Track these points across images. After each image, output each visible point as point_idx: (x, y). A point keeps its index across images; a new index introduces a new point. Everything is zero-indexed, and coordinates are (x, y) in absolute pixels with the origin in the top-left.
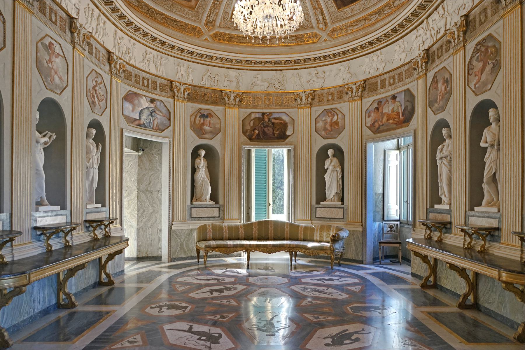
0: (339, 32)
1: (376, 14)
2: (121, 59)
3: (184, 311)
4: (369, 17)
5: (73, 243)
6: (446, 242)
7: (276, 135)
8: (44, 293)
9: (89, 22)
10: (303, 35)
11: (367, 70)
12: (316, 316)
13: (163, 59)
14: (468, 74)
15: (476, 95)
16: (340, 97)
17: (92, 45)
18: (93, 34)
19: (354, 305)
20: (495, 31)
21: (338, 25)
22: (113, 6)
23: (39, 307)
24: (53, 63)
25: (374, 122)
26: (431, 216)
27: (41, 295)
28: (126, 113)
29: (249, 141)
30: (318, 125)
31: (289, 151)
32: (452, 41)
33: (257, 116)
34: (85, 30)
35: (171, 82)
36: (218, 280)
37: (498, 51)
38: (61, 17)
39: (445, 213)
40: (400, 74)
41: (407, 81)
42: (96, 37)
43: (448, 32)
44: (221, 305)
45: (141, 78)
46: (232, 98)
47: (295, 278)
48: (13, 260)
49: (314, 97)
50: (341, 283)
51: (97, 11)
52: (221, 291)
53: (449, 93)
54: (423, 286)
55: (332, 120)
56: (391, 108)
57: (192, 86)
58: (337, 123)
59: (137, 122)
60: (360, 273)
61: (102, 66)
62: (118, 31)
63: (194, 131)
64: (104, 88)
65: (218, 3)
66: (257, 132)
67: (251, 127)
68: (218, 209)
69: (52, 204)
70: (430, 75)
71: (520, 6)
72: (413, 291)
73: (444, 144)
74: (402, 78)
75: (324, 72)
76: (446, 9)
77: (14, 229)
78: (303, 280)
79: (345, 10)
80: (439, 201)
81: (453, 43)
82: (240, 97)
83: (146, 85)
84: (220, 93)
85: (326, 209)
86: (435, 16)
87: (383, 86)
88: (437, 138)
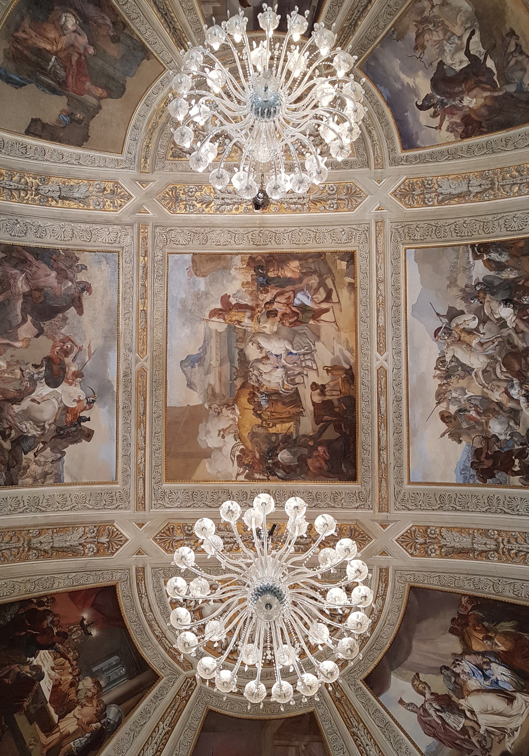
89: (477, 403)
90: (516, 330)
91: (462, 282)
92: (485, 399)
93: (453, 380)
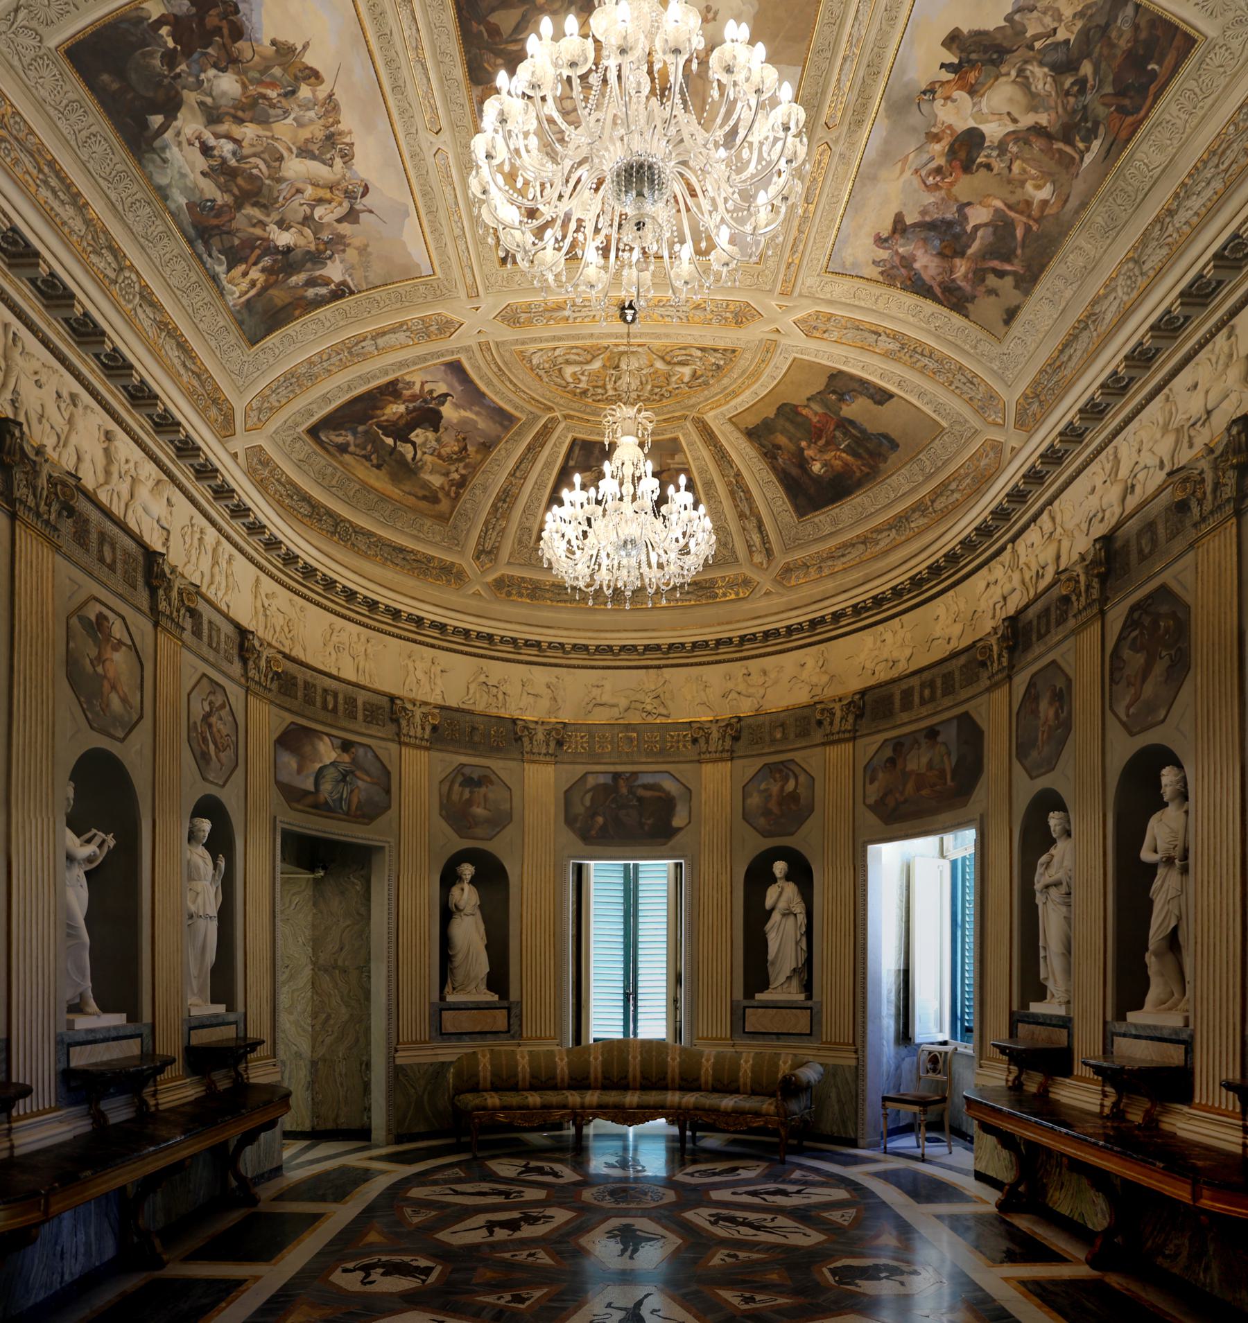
0: (801, 573)
1: (890, 529)
2: (269, 645)
3: (424, 1281)
4: (874, 536)
5: (157, 1105)
6: (1058, 1097)
7: (646, 828)
8: (87, 1234)
9: (193, 559)
10: (713, 582)
11: (869, 665)
12: (747, 1295)
13: (373, 641)
14: (1112, 680)
15: (1132, 734)
16: (804, 733)
17: (201, 616)
18: (204, 589)
19: (839, 1264)
20: (1175, 577)
21: (798, 555)
22: (251, 520)
23: (73, 1269)
24: (107, 663)
25: (885, 795)
26: (1023, 1029)
27: (81, 1236)
28: (284, 777)
29: (580, 845)
30: (749, 801)
31: (678, 866)
32: (1074, 598)
33: (602, 780)
34: (183, 581)
35: (392, 699)
36: (507, 1194)
37: (1182, 629)
38: (126, 553)
39: (1054, 1026)
40: (948, 677)
41: (964, 694)
42: (210, 594)
43: (1063, 577)
44: (511, 1266)
45: (319, 691)
46: (540, 736)
47: (694, 1188)
48: (12, 1156)
49: (738, 735)
50: (806, 1201)
51: (211, 533)
52: (513, 1225)
53: (1065, 726)
54: (1002, 1206)
55: (782, 788)
56: (924, 760)
57: (442, 708)
58: (794, 797)
59: (310, 800)
60: (852, 1172)
61: (225, 665)
62: (263, 577)
63: (447, 818)
64: (230, 718)
65: (505, 506)
66: (600, 820)
68: (505, 1012)
69: (105, 1008)
70: (1021, 681)
71: (1234, 520)
72: (980, 1219)
73: (1052, 851)
74: (953, 686)
75: (765, 673)
76: (1058, 520)
77: (14, 1080)
78: (715, 1195)
79: (816, 520)
80: (1040, 993)
81: (1076, 604)
82: (558, 734)
83: (330, 706)
84: (510, 726)
85: (770, 1011)
86: (1033, 535)
87: (907, 705)
88: (1036, 841)
89: (272, 111)
90: (263, 225)
91: (351, 254)
92: (263, 121)
93: (320, 135)
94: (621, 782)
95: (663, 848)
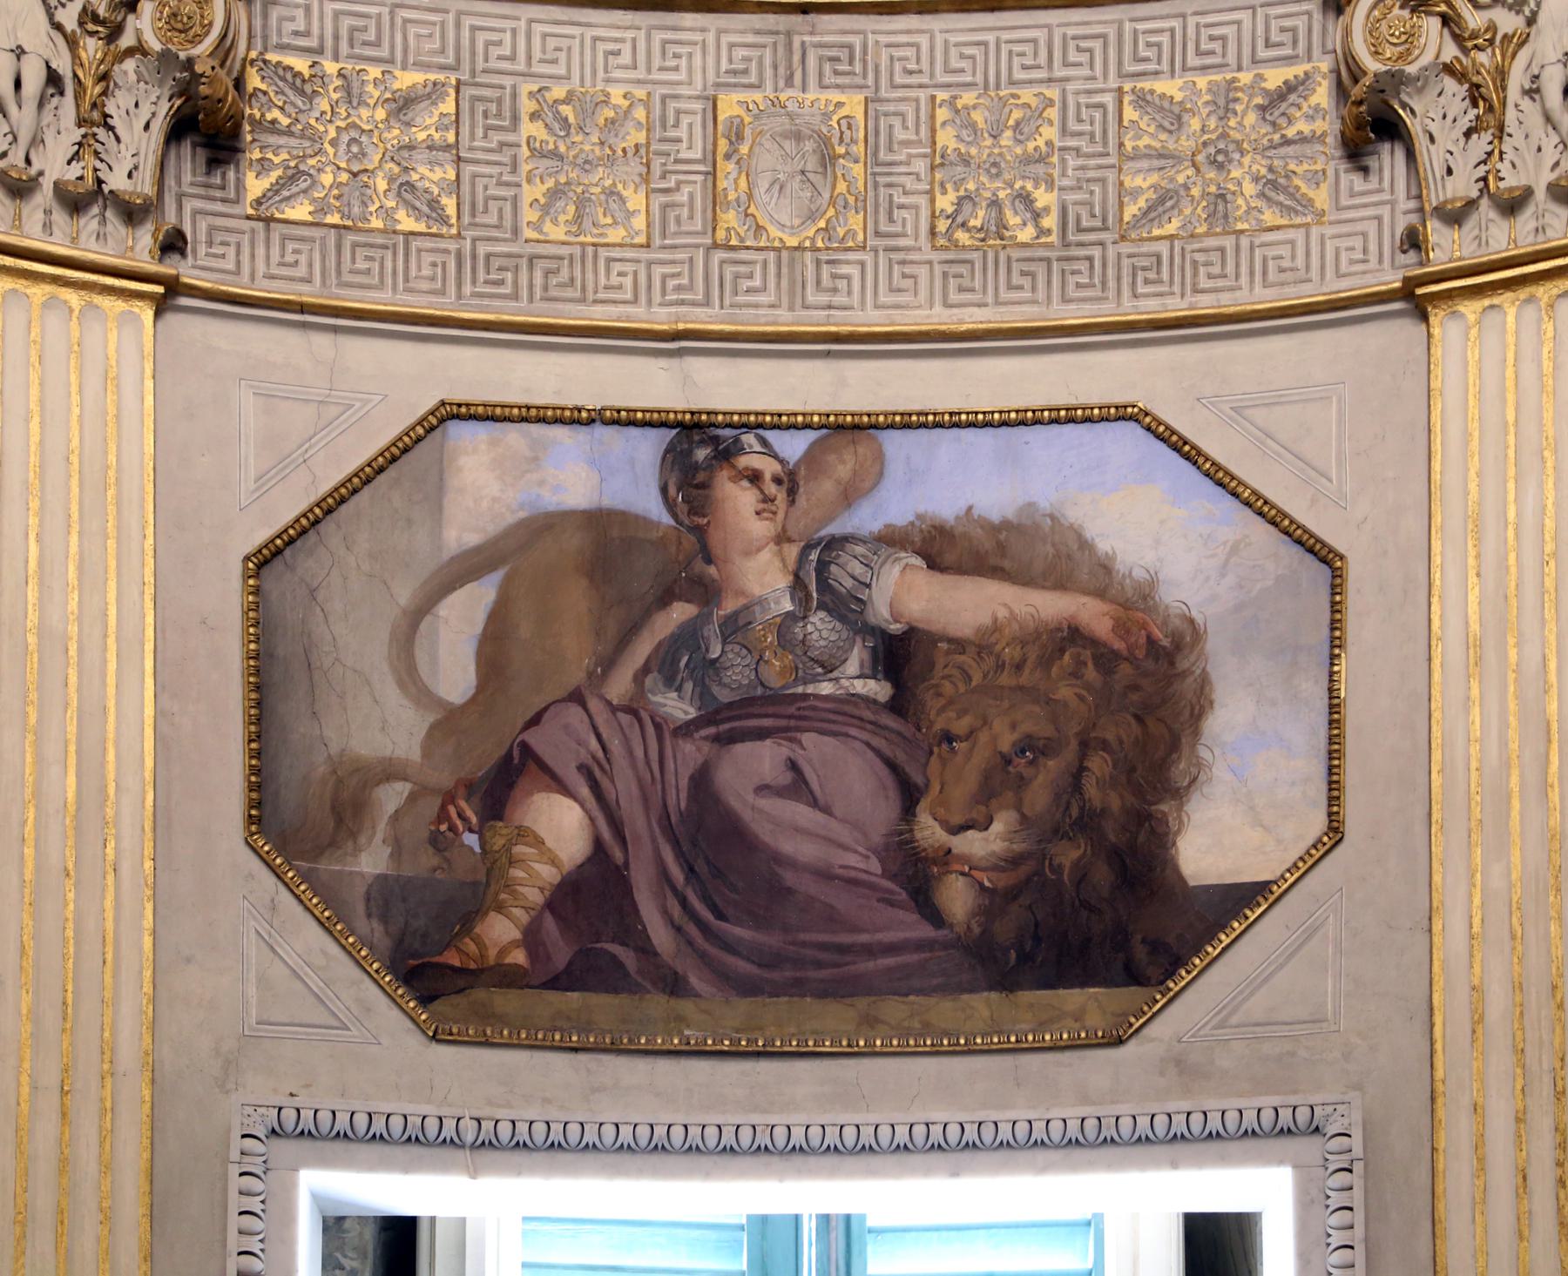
7: (957, 898)
29: (384, 1046)
66: (560, 826)
67: (449, 724)
94: (738, 503)
95: (1097, 1065)
